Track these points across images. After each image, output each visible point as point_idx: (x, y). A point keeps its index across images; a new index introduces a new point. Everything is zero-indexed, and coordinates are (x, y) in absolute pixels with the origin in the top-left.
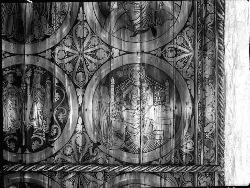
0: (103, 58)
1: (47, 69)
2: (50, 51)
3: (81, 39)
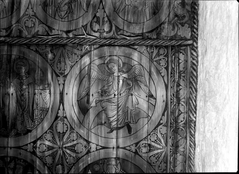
0: (81, 152)
1: (29, 161)
2: (32, 144)
3: (61, 134)
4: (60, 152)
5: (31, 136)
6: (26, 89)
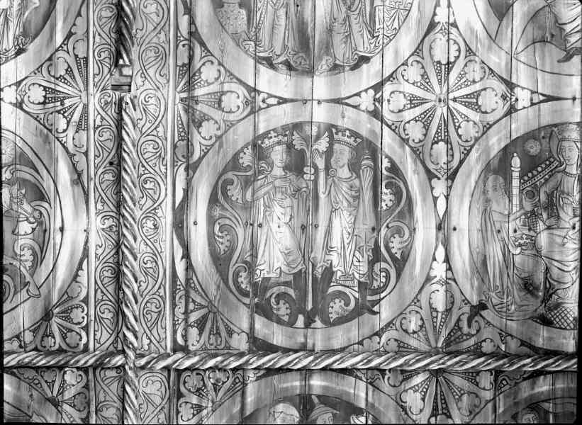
0: (494, 110)
1: (364, 133)
2: (371, 92)
3: (443, 67)
4: (441, 110)
5: (369, 71)
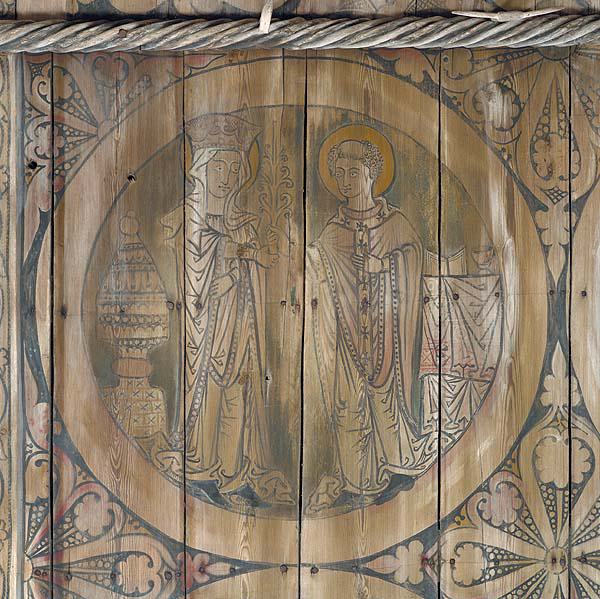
2: (417, 547)
3: (560, 495)
6: (382, 276)
